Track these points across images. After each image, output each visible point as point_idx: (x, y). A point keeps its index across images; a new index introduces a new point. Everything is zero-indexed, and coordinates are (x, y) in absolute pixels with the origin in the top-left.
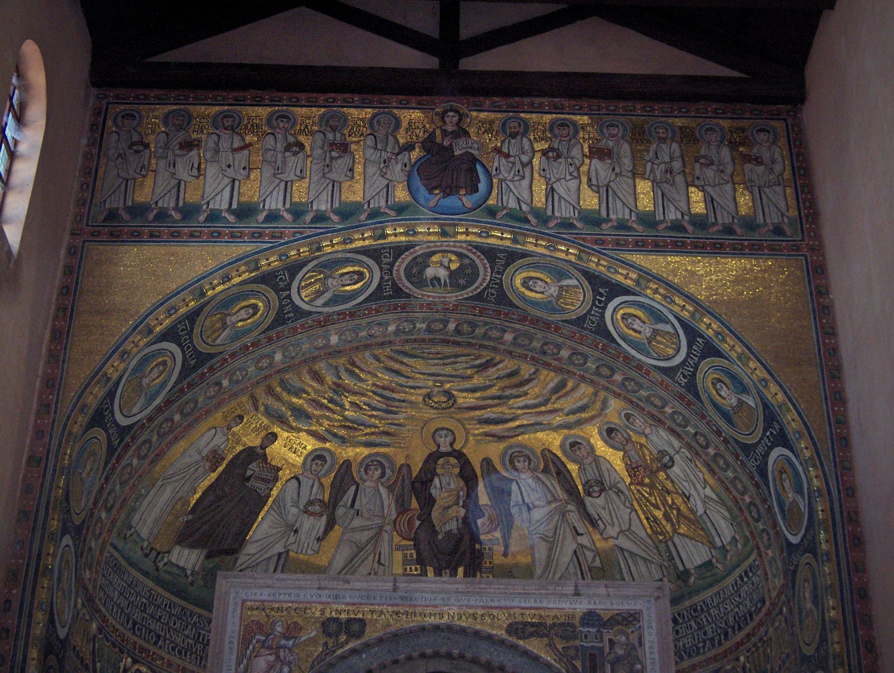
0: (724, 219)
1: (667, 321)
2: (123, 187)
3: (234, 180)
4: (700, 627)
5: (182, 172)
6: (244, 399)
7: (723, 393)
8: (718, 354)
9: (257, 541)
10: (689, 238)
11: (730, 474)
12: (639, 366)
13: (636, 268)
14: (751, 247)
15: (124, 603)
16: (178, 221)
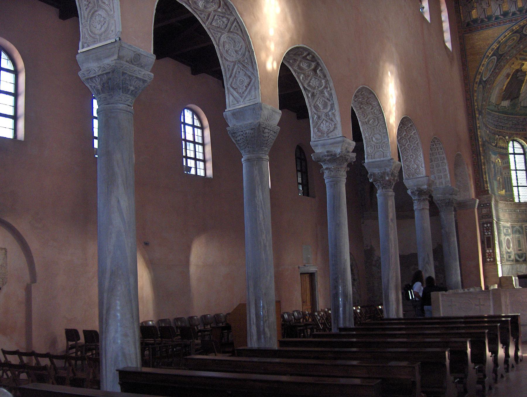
2: (469, 15)
3: (500, 5)
5: (484, 6)
6: (514, 59)
9: (524, 92)
15: (492, 122)
16: (486, 22)
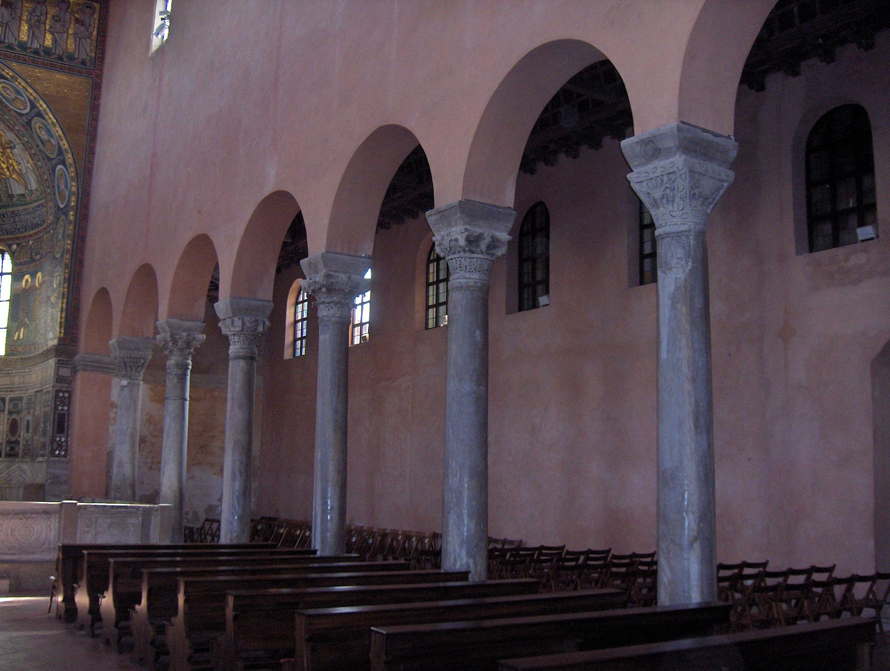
0: (59, 52)
1: (23, 97)
4: (15, 222)
7: (42, 132)
8: (44, 118)
10: (41, 59)
11: (40, 164)
12: (6, 107)
13: (13, 71)
14: (69, 69)
